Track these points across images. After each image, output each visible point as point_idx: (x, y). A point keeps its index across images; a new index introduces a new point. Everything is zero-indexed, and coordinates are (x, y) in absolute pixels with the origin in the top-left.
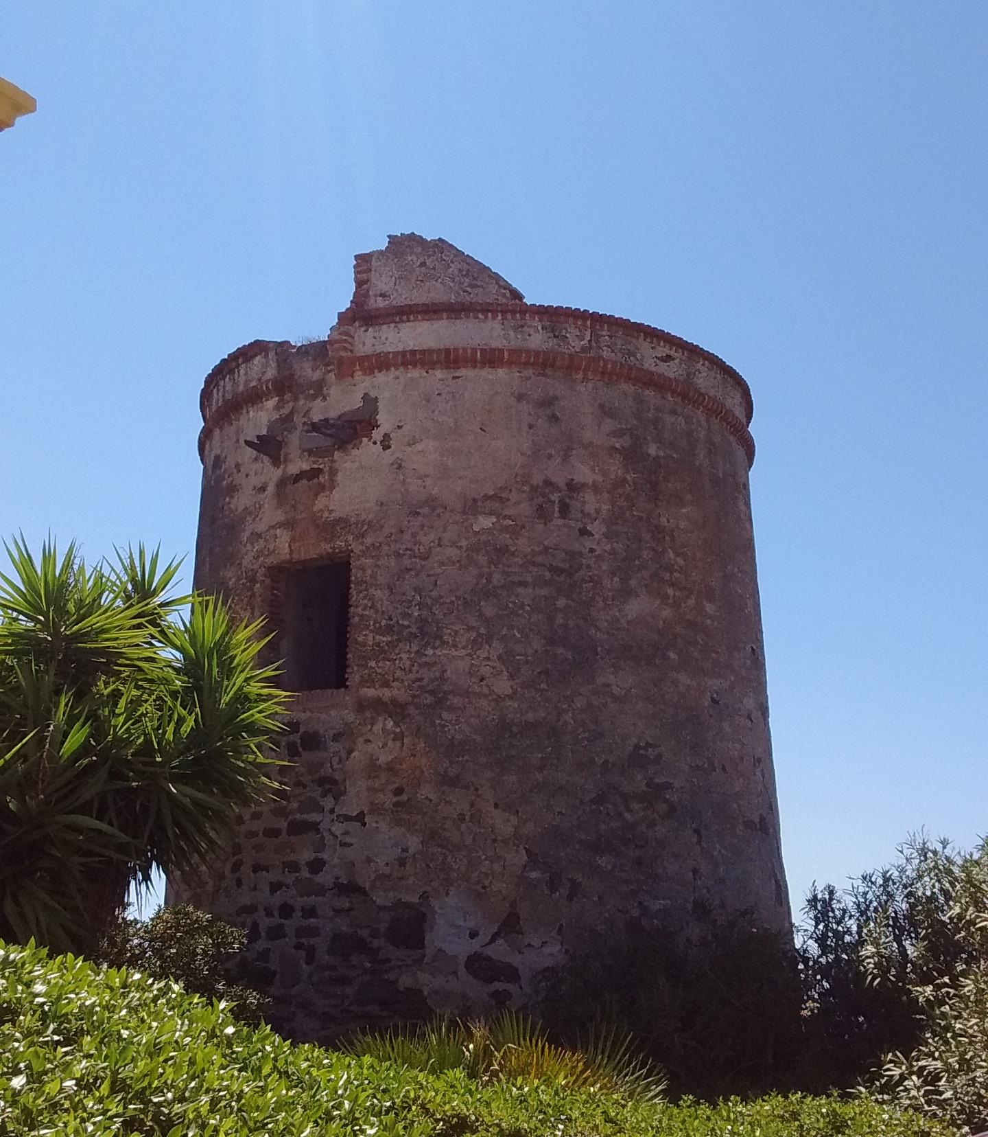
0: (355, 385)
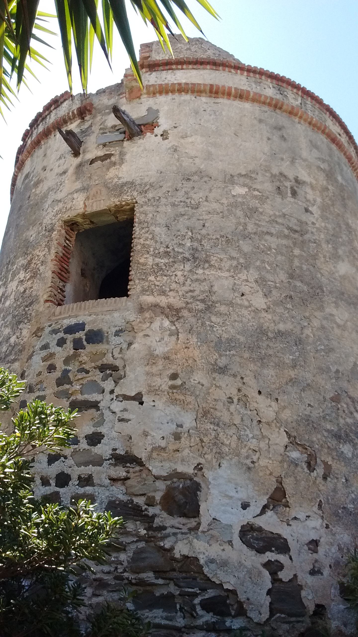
0: (141, 103)
